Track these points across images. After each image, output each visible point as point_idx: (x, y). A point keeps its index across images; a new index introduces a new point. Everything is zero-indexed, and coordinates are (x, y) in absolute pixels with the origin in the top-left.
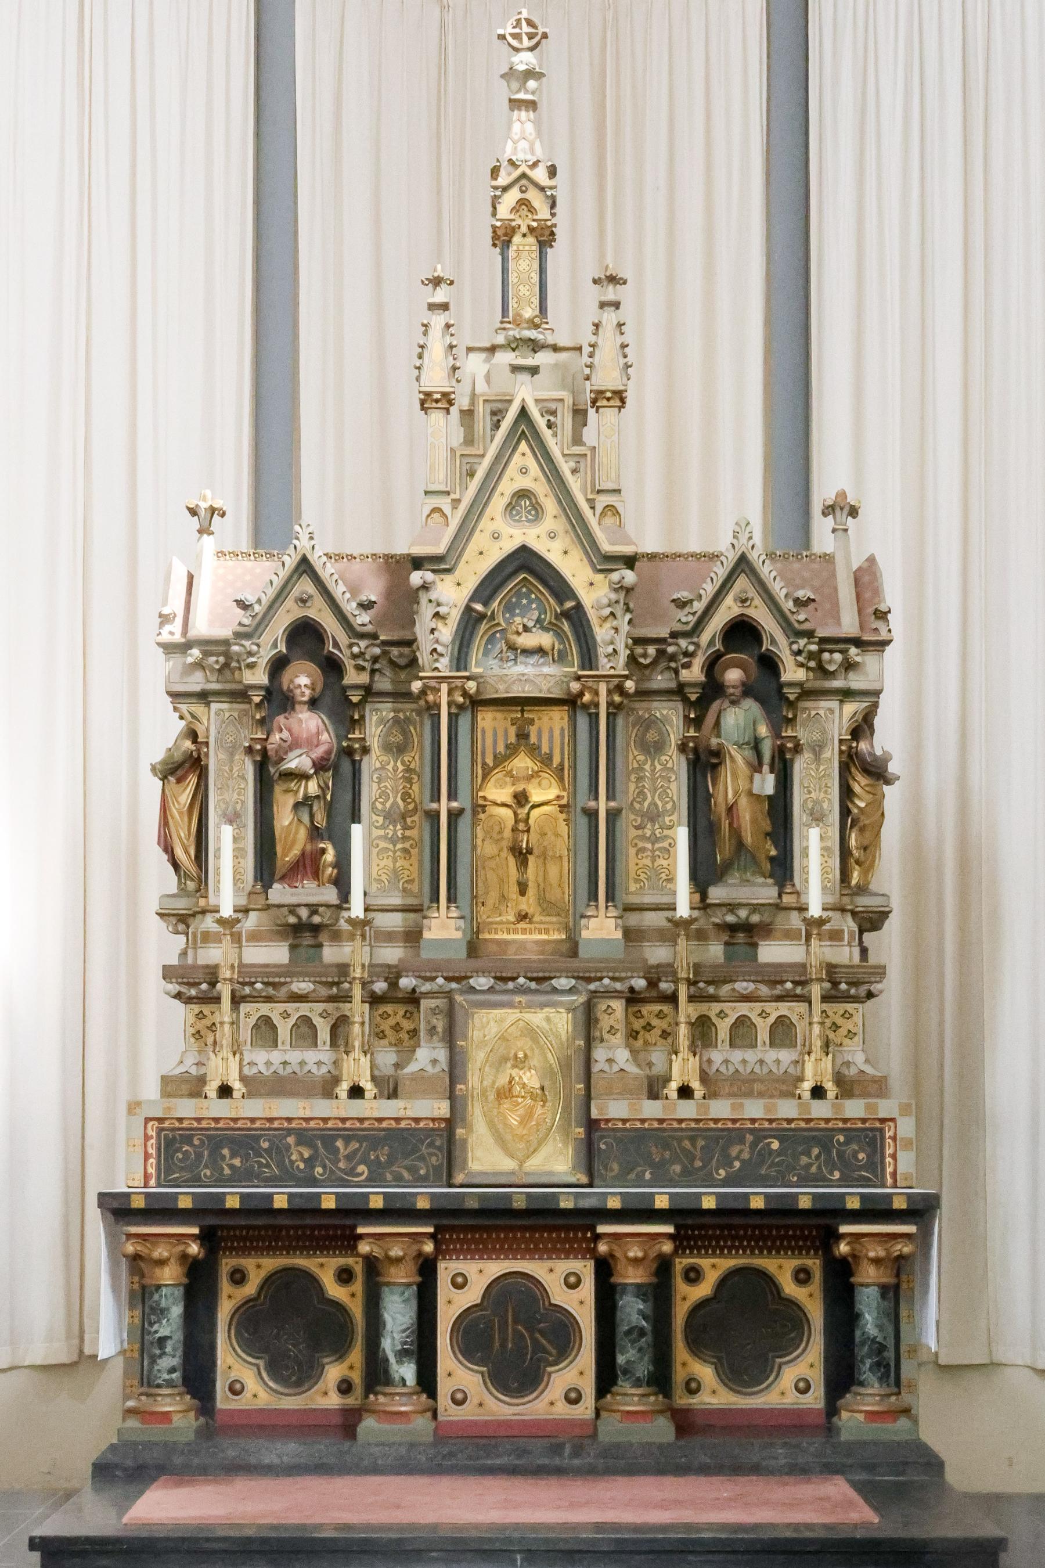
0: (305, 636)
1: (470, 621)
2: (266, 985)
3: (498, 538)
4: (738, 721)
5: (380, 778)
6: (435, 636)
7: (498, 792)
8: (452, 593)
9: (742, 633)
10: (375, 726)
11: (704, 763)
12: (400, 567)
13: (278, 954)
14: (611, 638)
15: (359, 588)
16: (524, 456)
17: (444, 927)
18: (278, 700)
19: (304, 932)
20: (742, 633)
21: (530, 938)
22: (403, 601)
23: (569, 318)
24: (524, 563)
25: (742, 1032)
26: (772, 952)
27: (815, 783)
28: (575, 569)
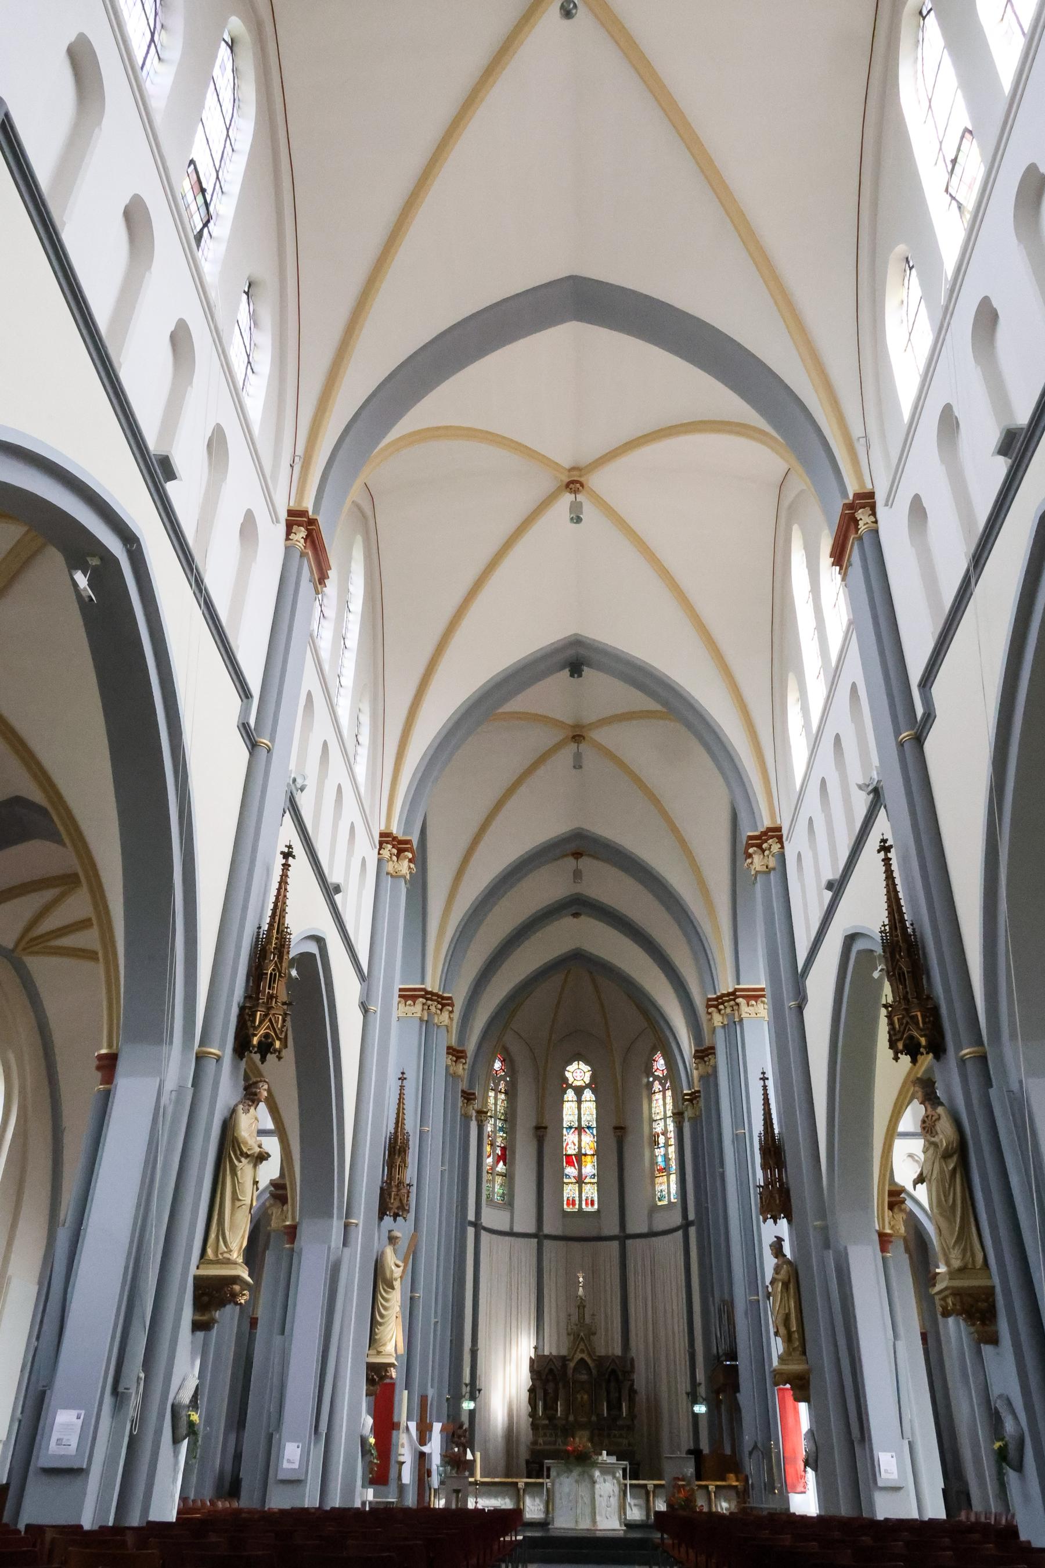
0: (551, 1370)
1: (575, 1369)
2: (545, 1427)
3: (579, 1356)
4: (613, 1384)
5: (562, 1393)
6: (570, 1372)
7: (579, 1396)
8: (572, 1365)
9: (613, 1372)
10: (561, 1385)
11: (608, 1393)
12: (564, 1359)
13: (547, 1422)
14: (594, 1372)
15: (559, 1364)
16: (582, 1343)
17: (571, 1418)
18: (547, 1381)
19: (551, 1418)
20: (613, 1372)
21: (584, 1420)
22: (564, 1366)
23: (588, 1320)
24: (582, 1359)
25: (615, 1436)
26: (620, 1423)
27: (625, 1393)
28: (589, 1361)
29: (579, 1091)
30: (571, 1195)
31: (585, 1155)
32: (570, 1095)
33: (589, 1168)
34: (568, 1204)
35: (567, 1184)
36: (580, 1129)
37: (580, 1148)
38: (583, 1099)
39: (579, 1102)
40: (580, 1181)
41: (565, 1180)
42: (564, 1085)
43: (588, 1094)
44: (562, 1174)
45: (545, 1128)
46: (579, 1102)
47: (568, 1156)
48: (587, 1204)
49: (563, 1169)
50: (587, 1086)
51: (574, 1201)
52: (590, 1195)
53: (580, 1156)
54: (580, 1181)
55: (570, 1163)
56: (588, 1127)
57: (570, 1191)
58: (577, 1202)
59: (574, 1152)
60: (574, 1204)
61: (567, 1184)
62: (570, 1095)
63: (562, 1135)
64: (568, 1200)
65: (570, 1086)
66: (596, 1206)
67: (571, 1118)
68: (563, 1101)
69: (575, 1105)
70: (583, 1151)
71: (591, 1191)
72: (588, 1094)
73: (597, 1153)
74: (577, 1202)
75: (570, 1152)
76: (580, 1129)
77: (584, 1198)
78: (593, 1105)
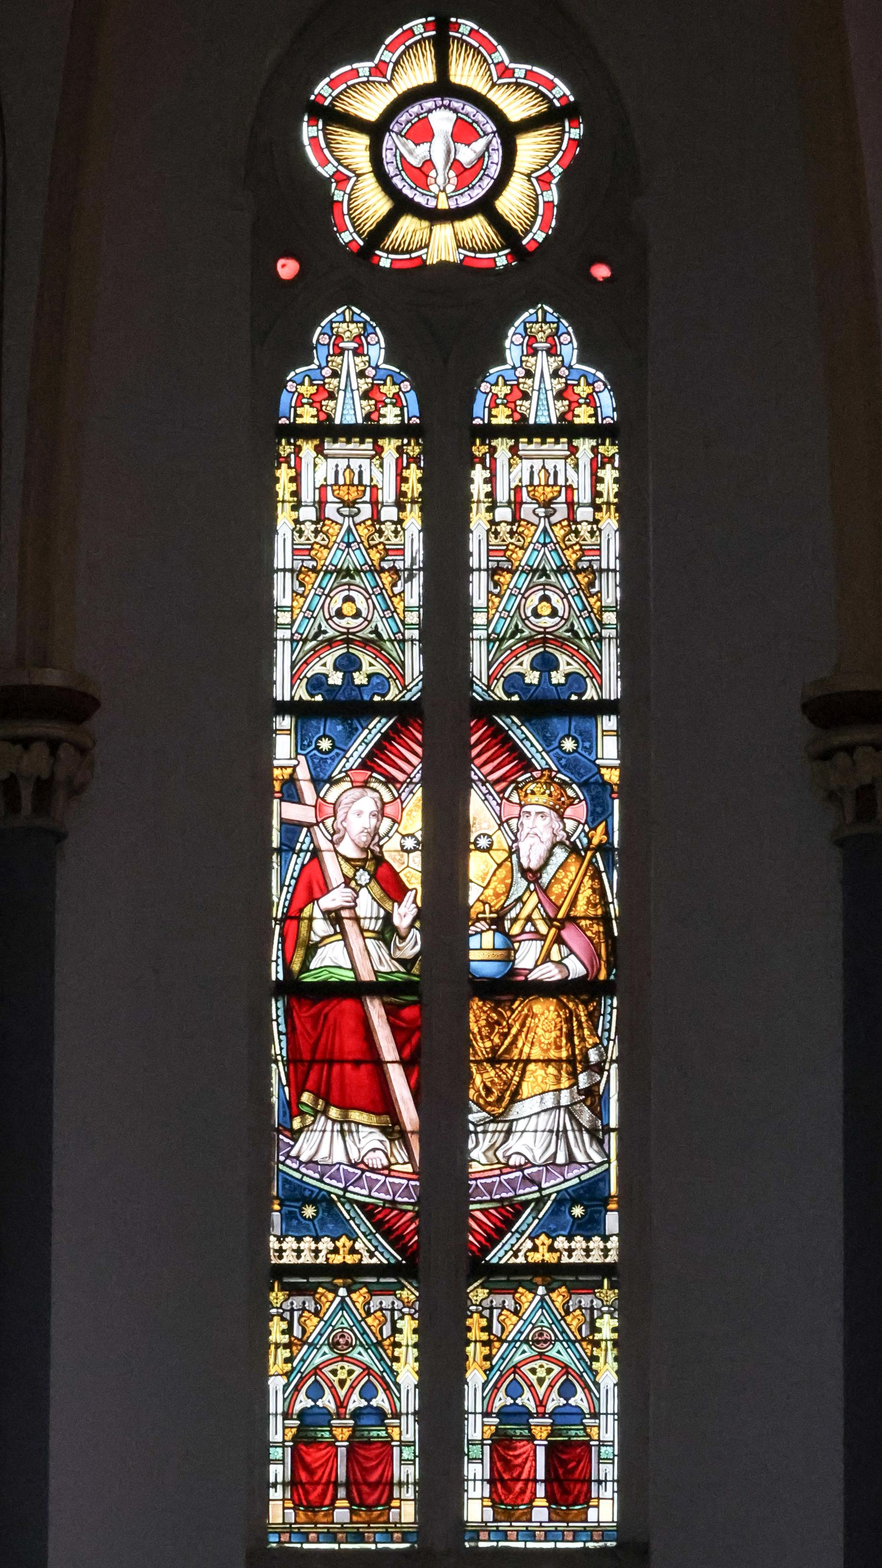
29: (444, 328)
30: (343, 1389)
31: (510, 988)
32: (350, 365)
33: (535, 1131)
34: (307, 1490)
35: (303, 1279)
36: (449, 731)
37: (446, 909)
38: (490, 405)
39: (447, 443)
40: (441, 1250)
41: (290, 1250)
42: (289, 259)
43: (539, 365)
44: (248, 1176)
45: (75, 706)
46: (447, 443)
47: (311, 997)
48: (506, 1485)
49: (263, 1137)
50: (531, 274)
51: (369, 1461)
52: (539, 1390)
53: (443, 1001)
54: (441, 1250)
55: (340, 1078)
56: (543, 708)
57: (332, 1358)
58: (406, 1470)
59: (374, 961)
60: (369, 1484)
61: (303, 1279)
62: (350, 365)
63: (259, 786)
64: (308, 1426)
65: (357, 276)
66: (605, 1510)
67: (359, 610)
68: (271, 435)
69: (386, 471)
70: (482, 951)
71: (555, 1358)
72: (539, 365)
73: (628, 975)
74: (406, 1470)
75: (332, 960)
76: (449, 731)
77: (476, 1429)
78: (585, 474)
